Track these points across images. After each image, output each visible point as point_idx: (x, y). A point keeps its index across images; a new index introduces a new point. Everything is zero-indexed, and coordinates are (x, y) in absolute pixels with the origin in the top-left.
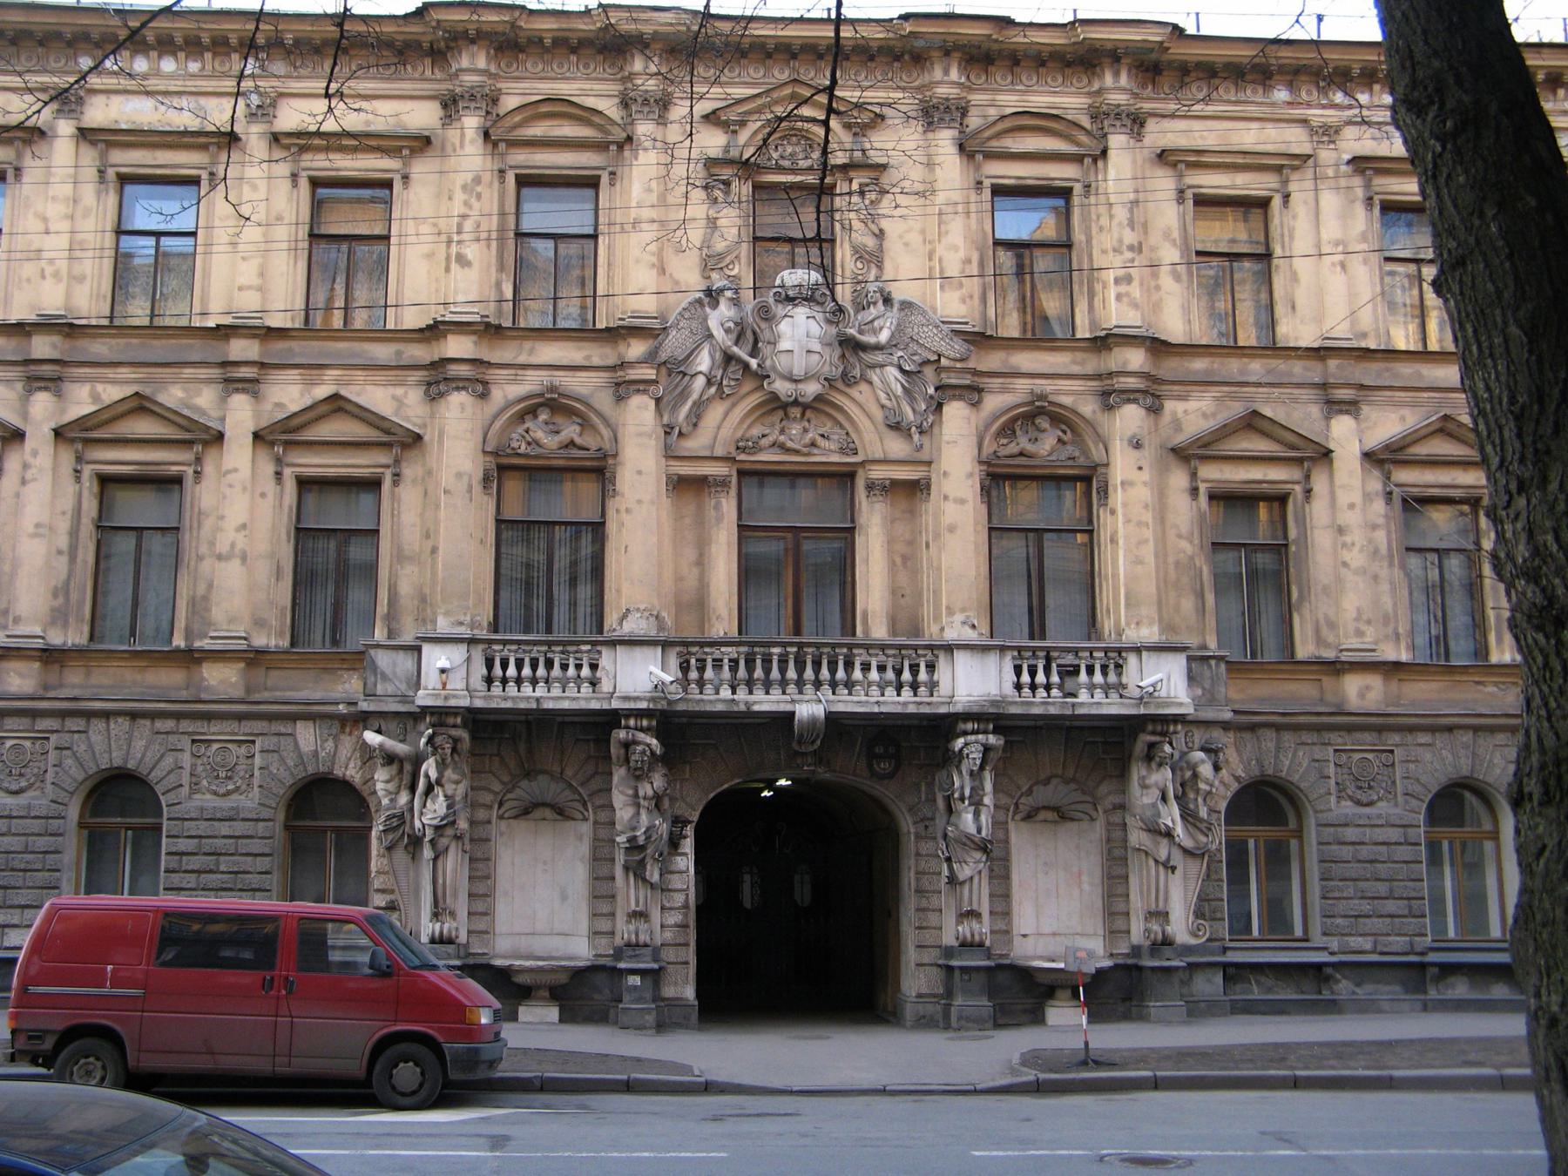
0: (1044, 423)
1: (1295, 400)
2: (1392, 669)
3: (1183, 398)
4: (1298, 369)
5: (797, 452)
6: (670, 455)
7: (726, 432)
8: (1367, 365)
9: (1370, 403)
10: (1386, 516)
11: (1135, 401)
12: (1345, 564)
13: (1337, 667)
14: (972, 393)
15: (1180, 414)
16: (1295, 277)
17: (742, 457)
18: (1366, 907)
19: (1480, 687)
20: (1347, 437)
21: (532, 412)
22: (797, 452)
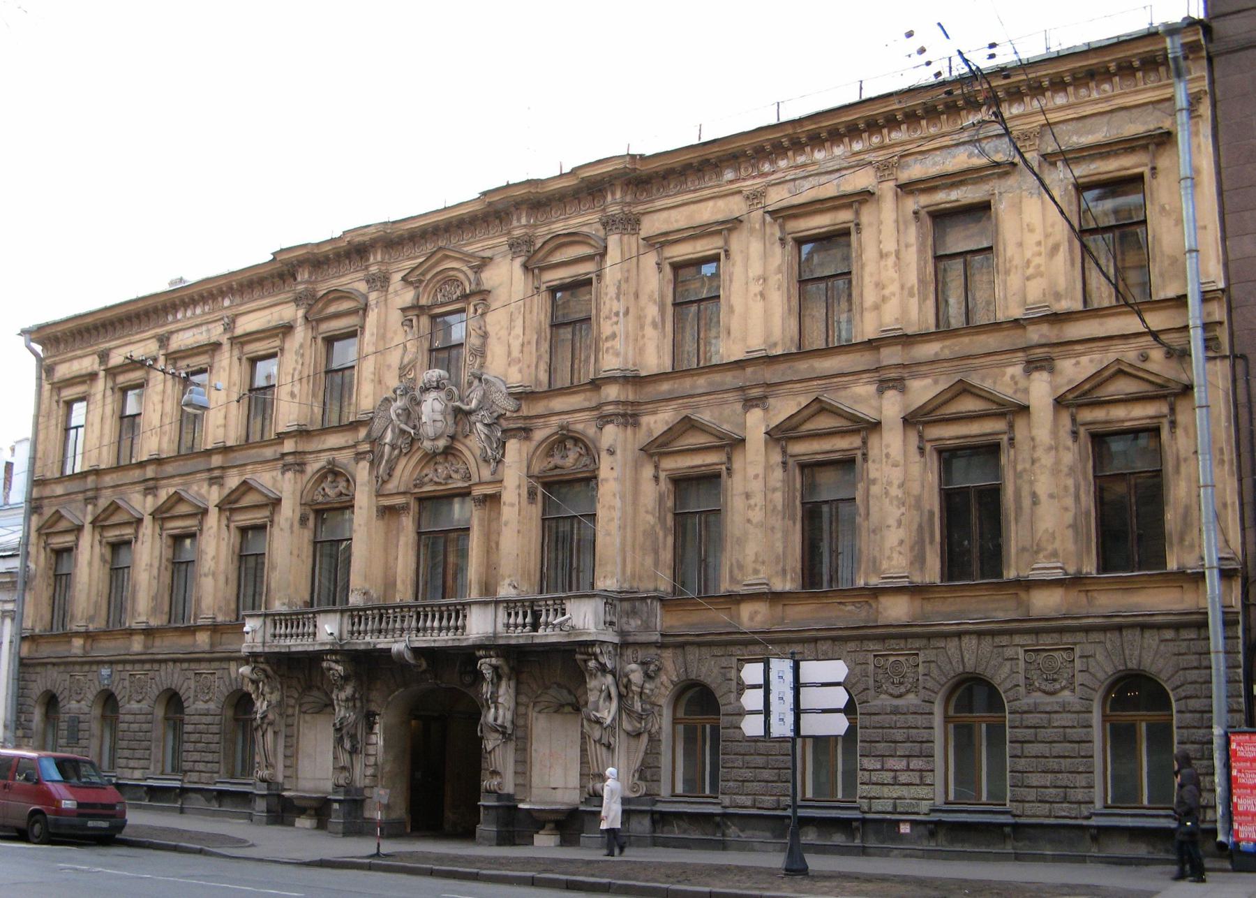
0: (569, 444)
1: (726, 402)
2: (775, 597)
3: (654, 413)
4: (729, 379)
5: (440, 484)
6: (379, 495)
7: (407, 473)
8: (776, 367)
9: (777, 396)
10: (783, 481)
11: (612, 422)
12: (749, 521)
13: (735, 599)
14: (525, 432)
15: (652, 425)
16: (731, 310)
17: (416, 490)
18: (748, 774)
19: (842, 607)
20: (756, 424)
21: (324, 477)
22: (440, 484)
